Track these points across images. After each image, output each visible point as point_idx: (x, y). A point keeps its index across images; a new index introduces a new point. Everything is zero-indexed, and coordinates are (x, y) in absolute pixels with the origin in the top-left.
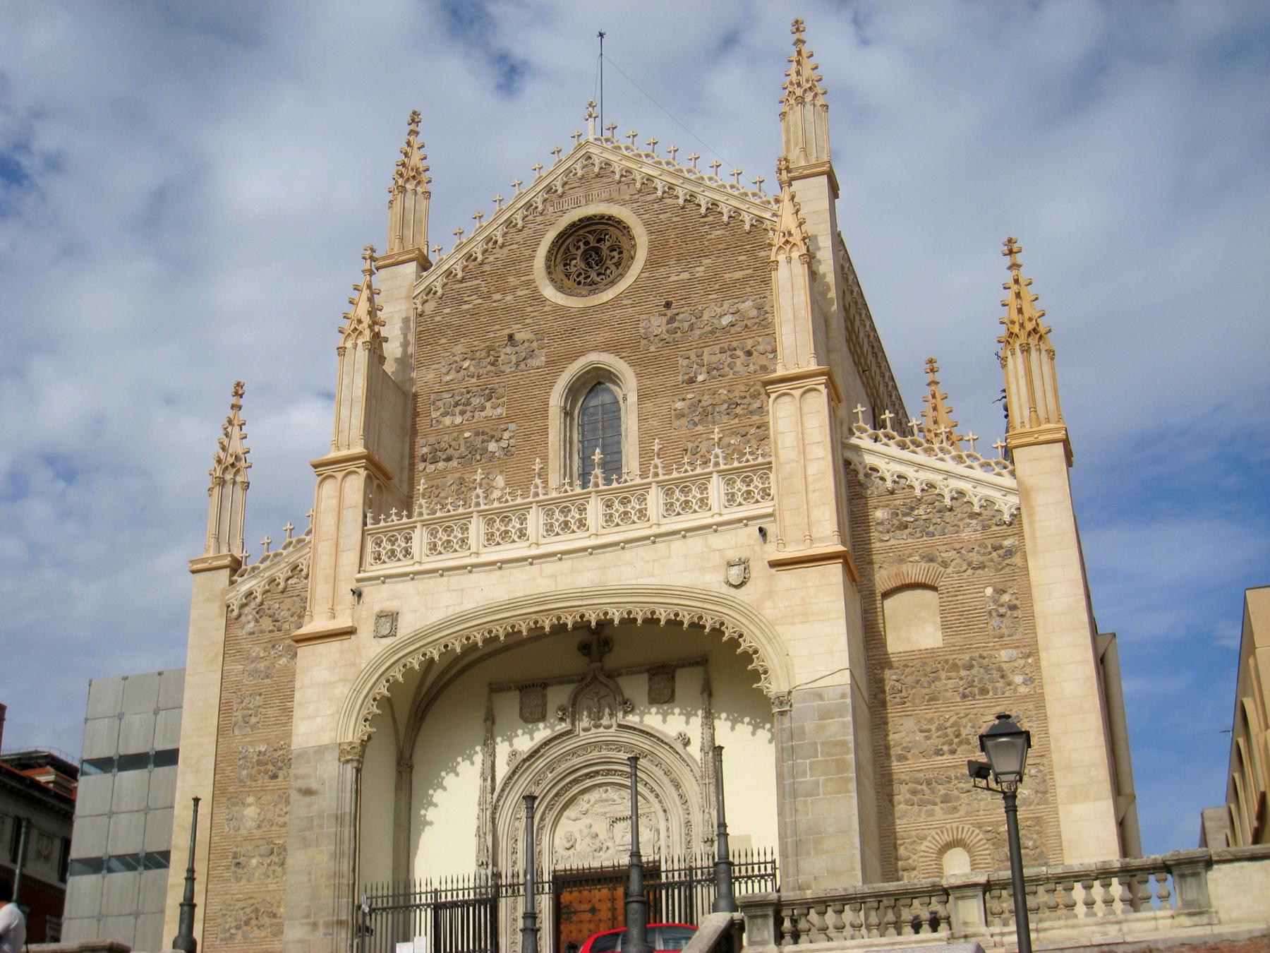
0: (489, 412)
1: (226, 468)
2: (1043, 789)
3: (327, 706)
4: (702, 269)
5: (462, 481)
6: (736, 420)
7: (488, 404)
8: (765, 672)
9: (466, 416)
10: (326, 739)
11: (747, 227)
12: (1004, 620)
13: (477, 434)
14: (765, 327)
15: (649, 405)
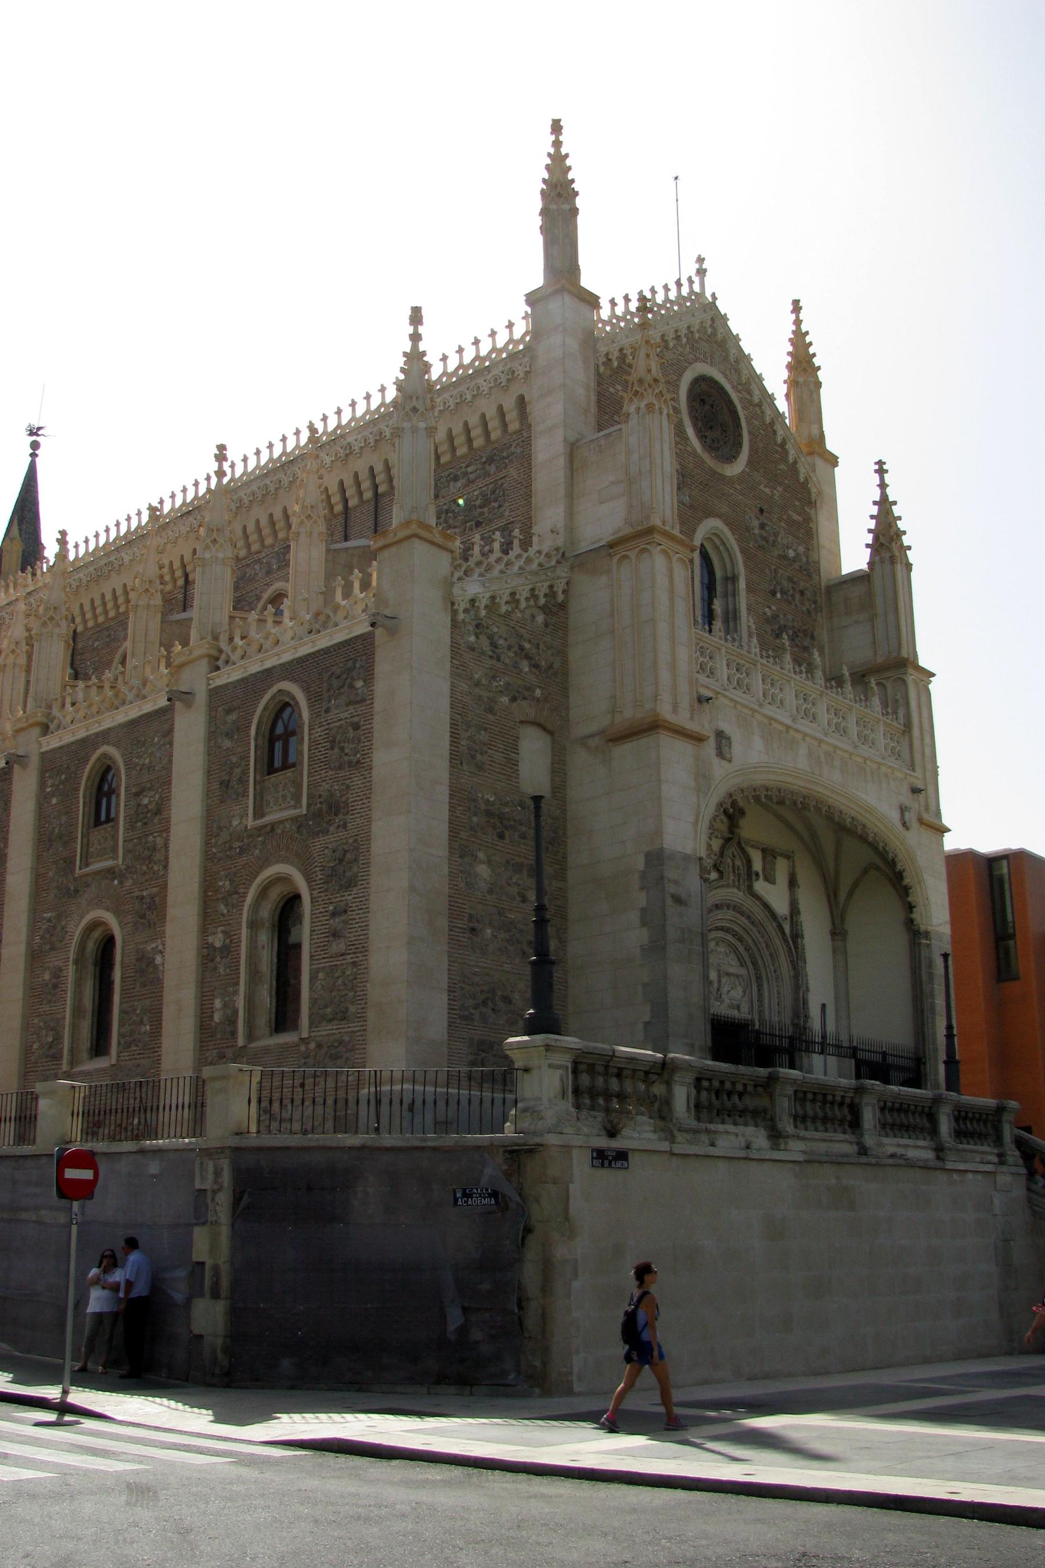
6: (796, 649)
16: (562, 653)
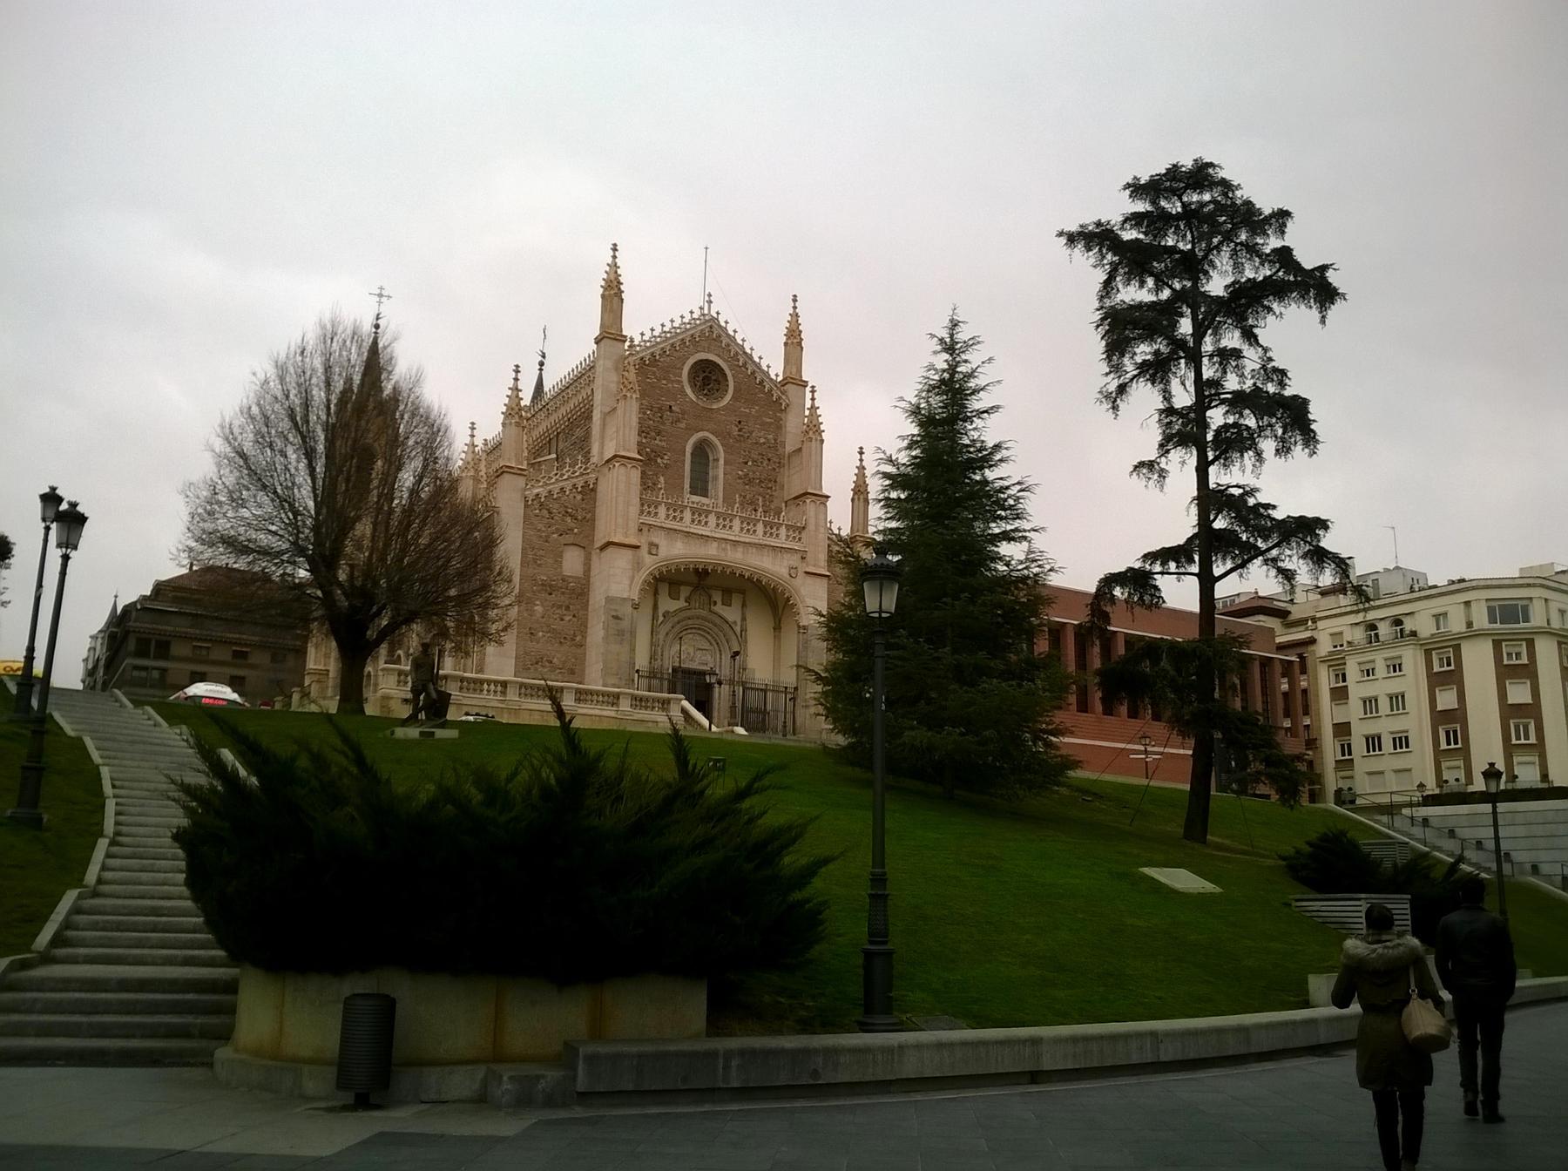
16: (593, 511)
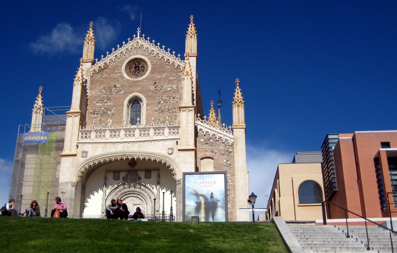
0: (108, 104)
1: (38, 109)
2: (233, 206)
3: (68, 173)
4: (164, 75)
5: (101, 120)
6: (170, 114)
7: (108, 102)
8: (175, 174)
9: (103, 104)
10: (68, 180)
11: (176, 67)
12: (228, 167)
13: (105, 109)
14: (178, 92)
15: (149, 107)
